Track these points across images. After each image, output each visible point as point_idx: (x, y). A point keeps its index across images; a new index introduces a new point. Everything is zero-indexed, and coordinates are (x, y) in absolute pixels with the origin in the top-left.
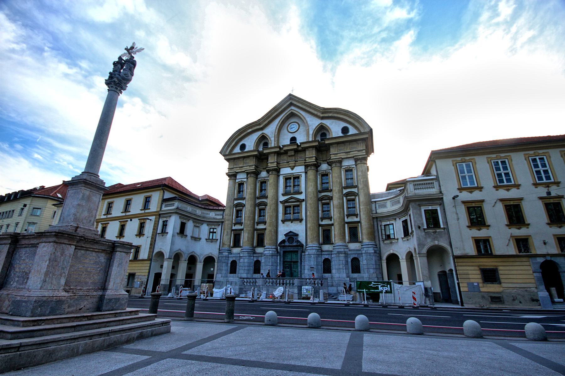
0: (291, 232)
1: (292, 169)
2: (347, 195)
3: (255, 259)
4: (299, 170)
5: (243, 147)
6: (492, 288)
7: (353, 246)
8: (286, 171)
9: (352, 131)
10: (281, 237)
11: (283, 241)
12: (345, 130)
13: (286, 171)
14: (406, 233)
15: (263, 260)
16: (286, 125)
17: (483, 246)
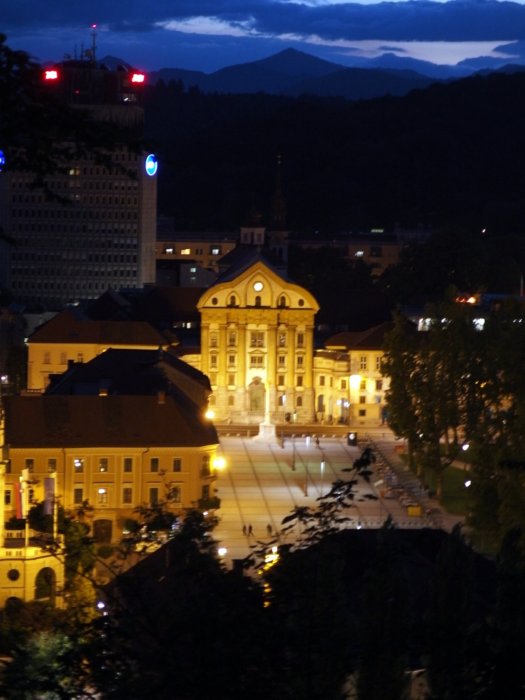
0: (257, 377)
1: (258, 326)
2: (298, 353)
3: (230, 395)
4: (263, 327)
5: (215, 301)
6: (362, 418)
7: (299, 389)
8: (252, 327)
9: (306, 305)
10: (249, 380)
11: (251, 384)
12: (301, 302)
13: (252, 327)
14: (331, 385)
15: (236, 396)
16: (252, 283)
17: (363, 400)
